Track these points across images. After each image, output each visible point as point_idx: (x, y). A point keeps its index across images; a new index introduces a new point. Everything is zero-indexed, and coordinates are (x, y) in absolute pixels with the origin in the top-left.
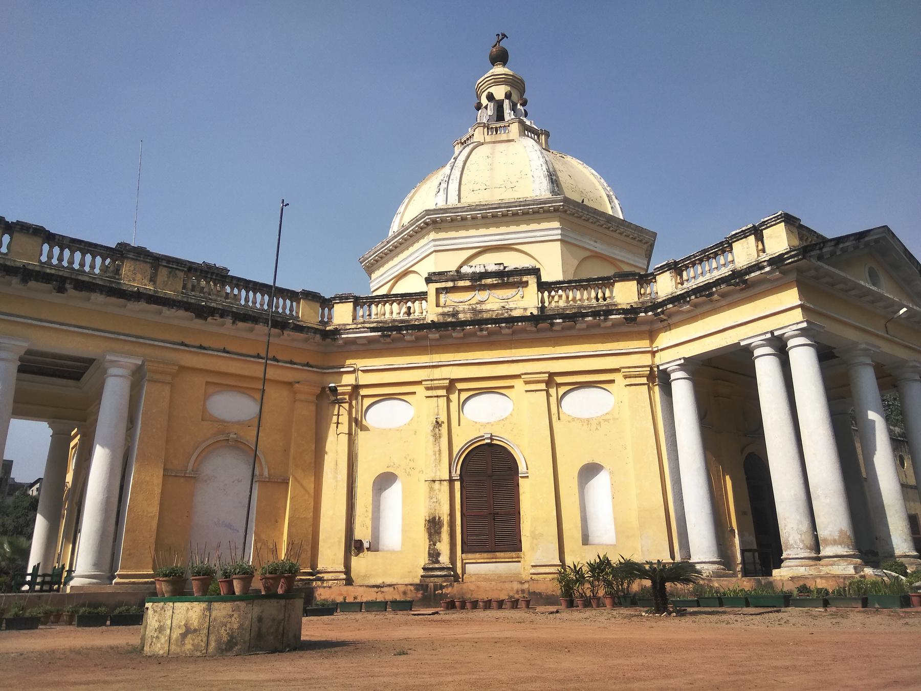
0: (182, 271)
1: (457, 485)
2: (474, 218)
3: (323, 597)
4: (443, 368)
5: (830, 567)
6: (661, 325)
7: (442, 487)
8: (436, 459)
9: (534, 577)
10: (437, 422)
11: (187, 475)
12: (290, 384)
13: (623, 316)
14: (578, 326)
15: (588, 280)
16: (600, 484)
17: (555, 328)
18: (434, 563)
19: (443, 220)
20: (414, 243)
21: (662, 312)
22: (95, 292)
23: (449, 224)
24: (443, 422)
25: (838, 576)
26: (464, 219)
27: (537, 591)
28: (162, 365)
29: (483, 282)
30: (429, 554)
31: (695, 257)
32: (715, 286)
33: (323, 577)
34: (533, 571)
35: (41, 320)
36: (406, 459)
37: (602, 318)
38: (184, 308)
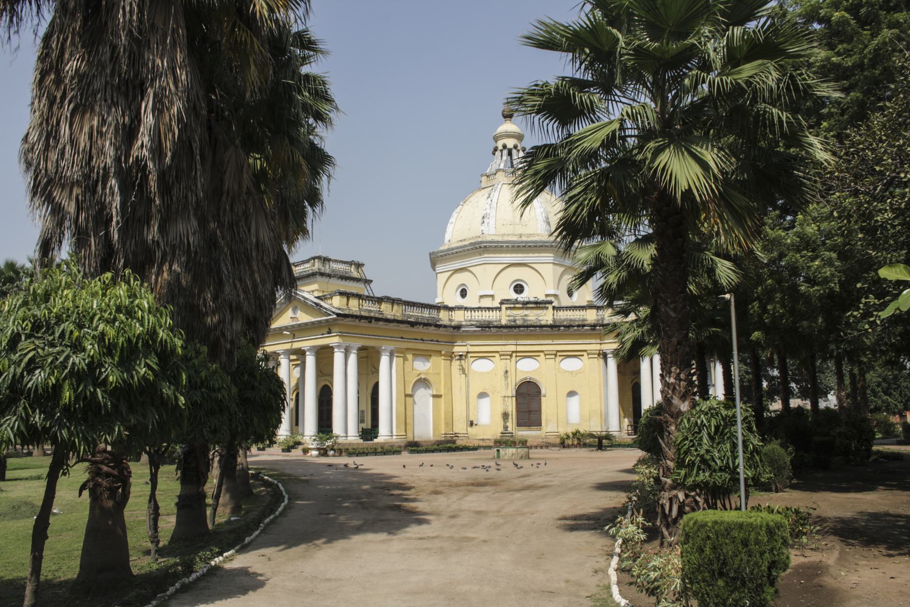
1: (514, 398)
2: (507, 247)
16: (574, 400)
19: (490, 246)
26: (502, 247)
29: (528, 306)
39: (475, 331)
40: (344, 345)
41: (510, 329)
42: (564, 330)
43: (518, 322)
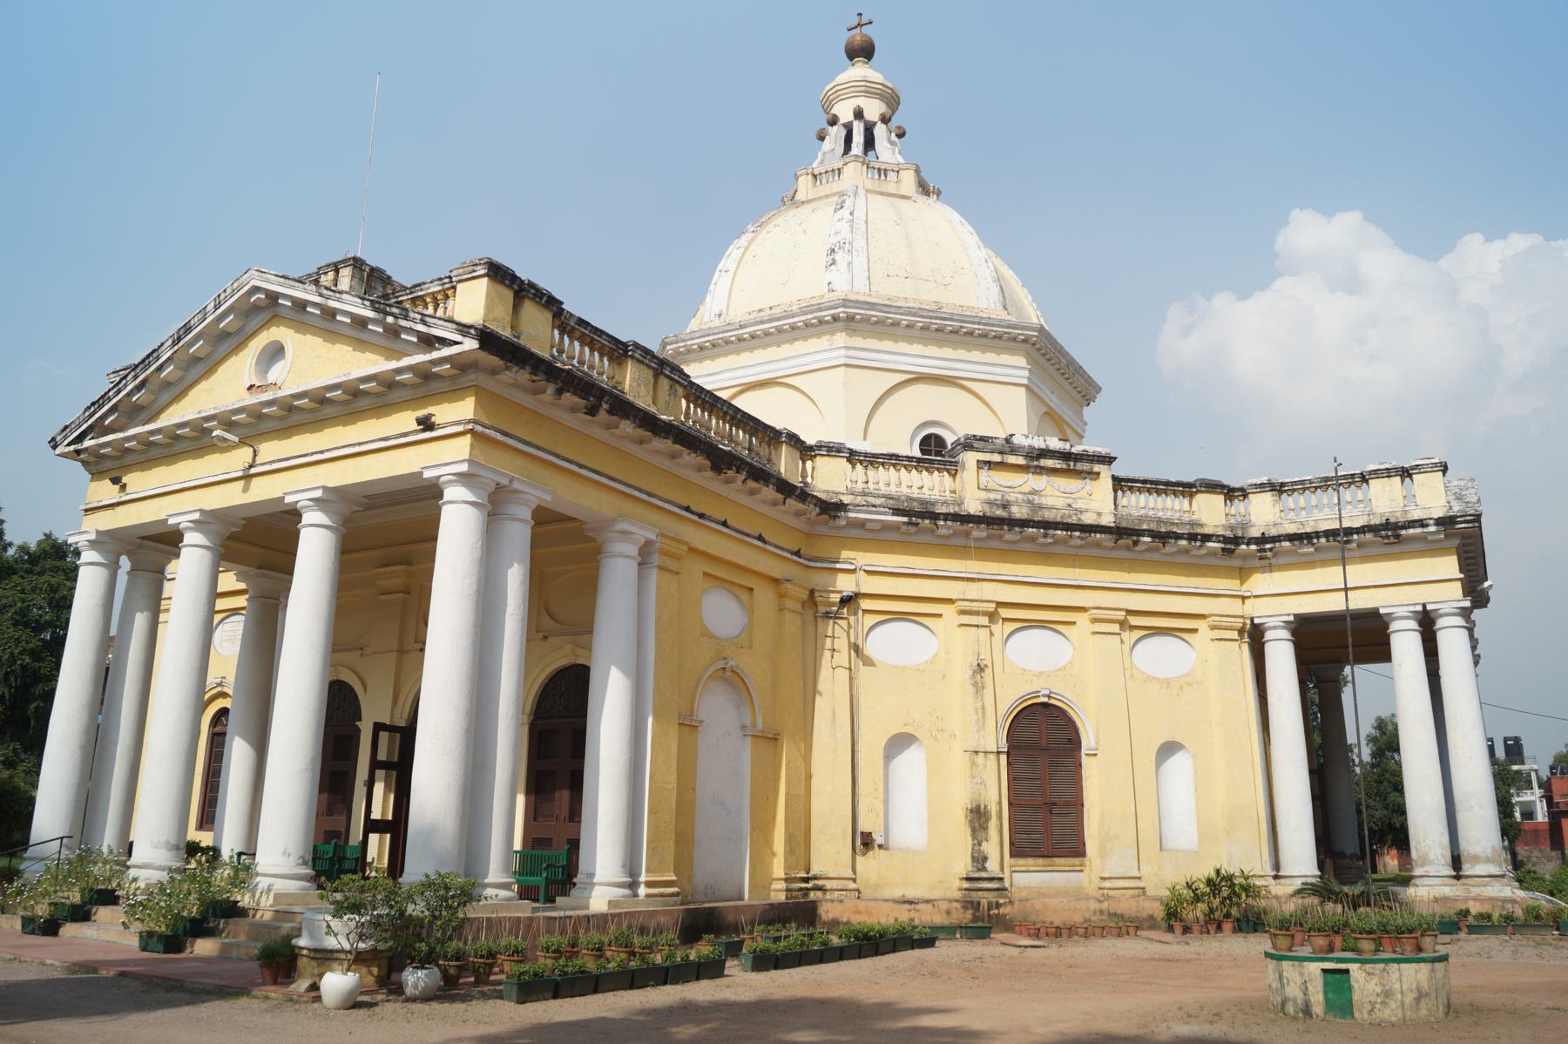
0: (681, 384)
1: (1004, 758)
3: (831, 916)
4: (985, 584)
5: (1483, 888)
6: (1258, 563)
7: (988, 761)
8: (978, 720)
9: (1111, 892)
10: (979, 665)
11: (693, 724)
12: (776, 581)
13: (1222, 545)
14: (1168, 549)
15: (1168, 483)
17: (1139, 548)
18: (979, 870)
19: (866, 320)
20: (796, 340)
21: (1271, 549)
22: (629, 419)
23: (871, 326)
24: (986, 666)
25: (1496, 899)
26: (896, 324)
27: (1119, 912)
28: (673, 544)
30: (973, 858)
31: (1311, 483)
32: (1358, 533)
33: (824, 886)
34: (1107, 884)
35: (558, 456)
36: (931, 716)
37: (1198, 544)
38: (707, 453)
39: (886, 526)
40: (491, 478)
41: (995, 531)
42: (1150, 550)
43: (1014, 509)
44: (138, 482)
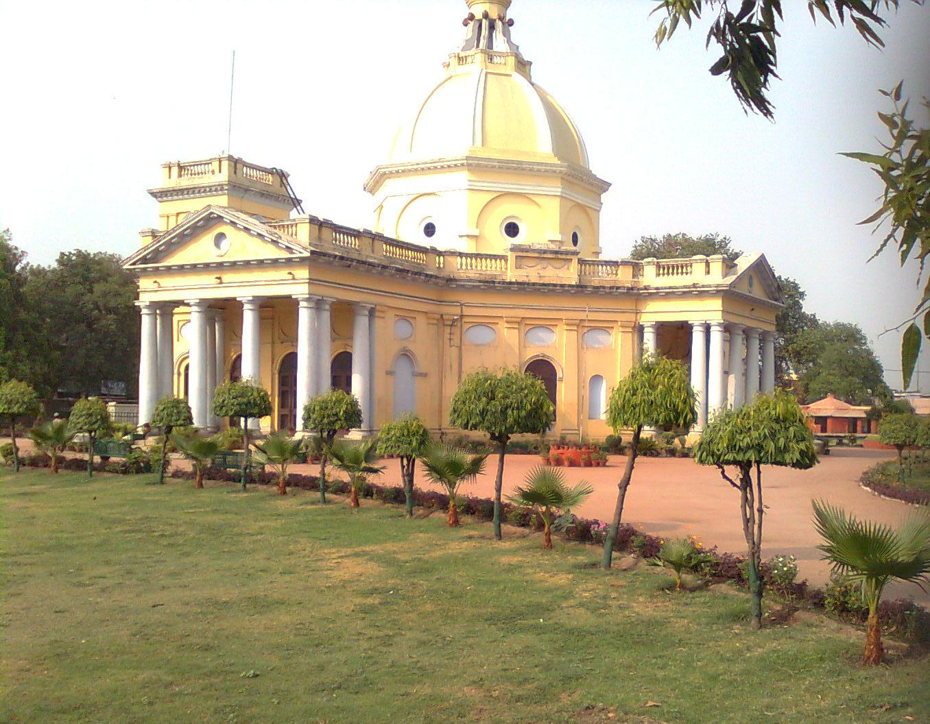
12: (426, 313)
29: (545, 256)
34: (563, 432)
44: (166, 281)
